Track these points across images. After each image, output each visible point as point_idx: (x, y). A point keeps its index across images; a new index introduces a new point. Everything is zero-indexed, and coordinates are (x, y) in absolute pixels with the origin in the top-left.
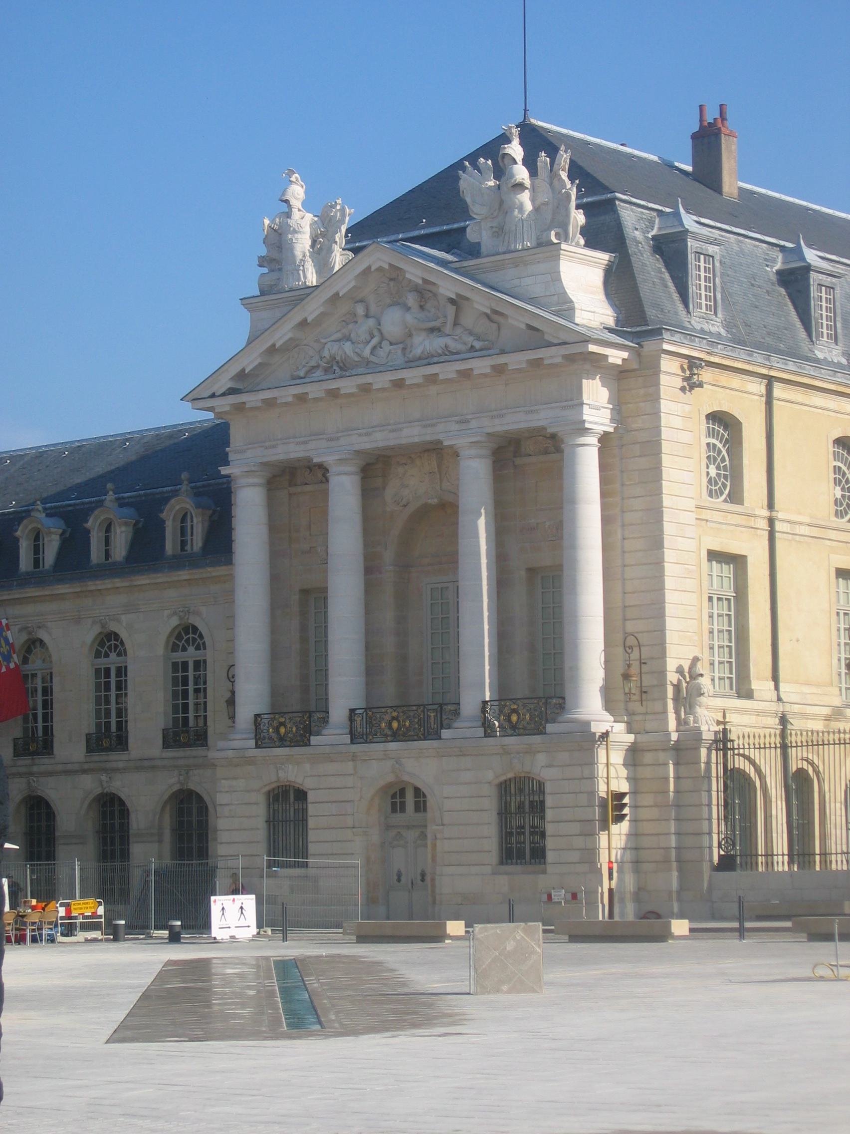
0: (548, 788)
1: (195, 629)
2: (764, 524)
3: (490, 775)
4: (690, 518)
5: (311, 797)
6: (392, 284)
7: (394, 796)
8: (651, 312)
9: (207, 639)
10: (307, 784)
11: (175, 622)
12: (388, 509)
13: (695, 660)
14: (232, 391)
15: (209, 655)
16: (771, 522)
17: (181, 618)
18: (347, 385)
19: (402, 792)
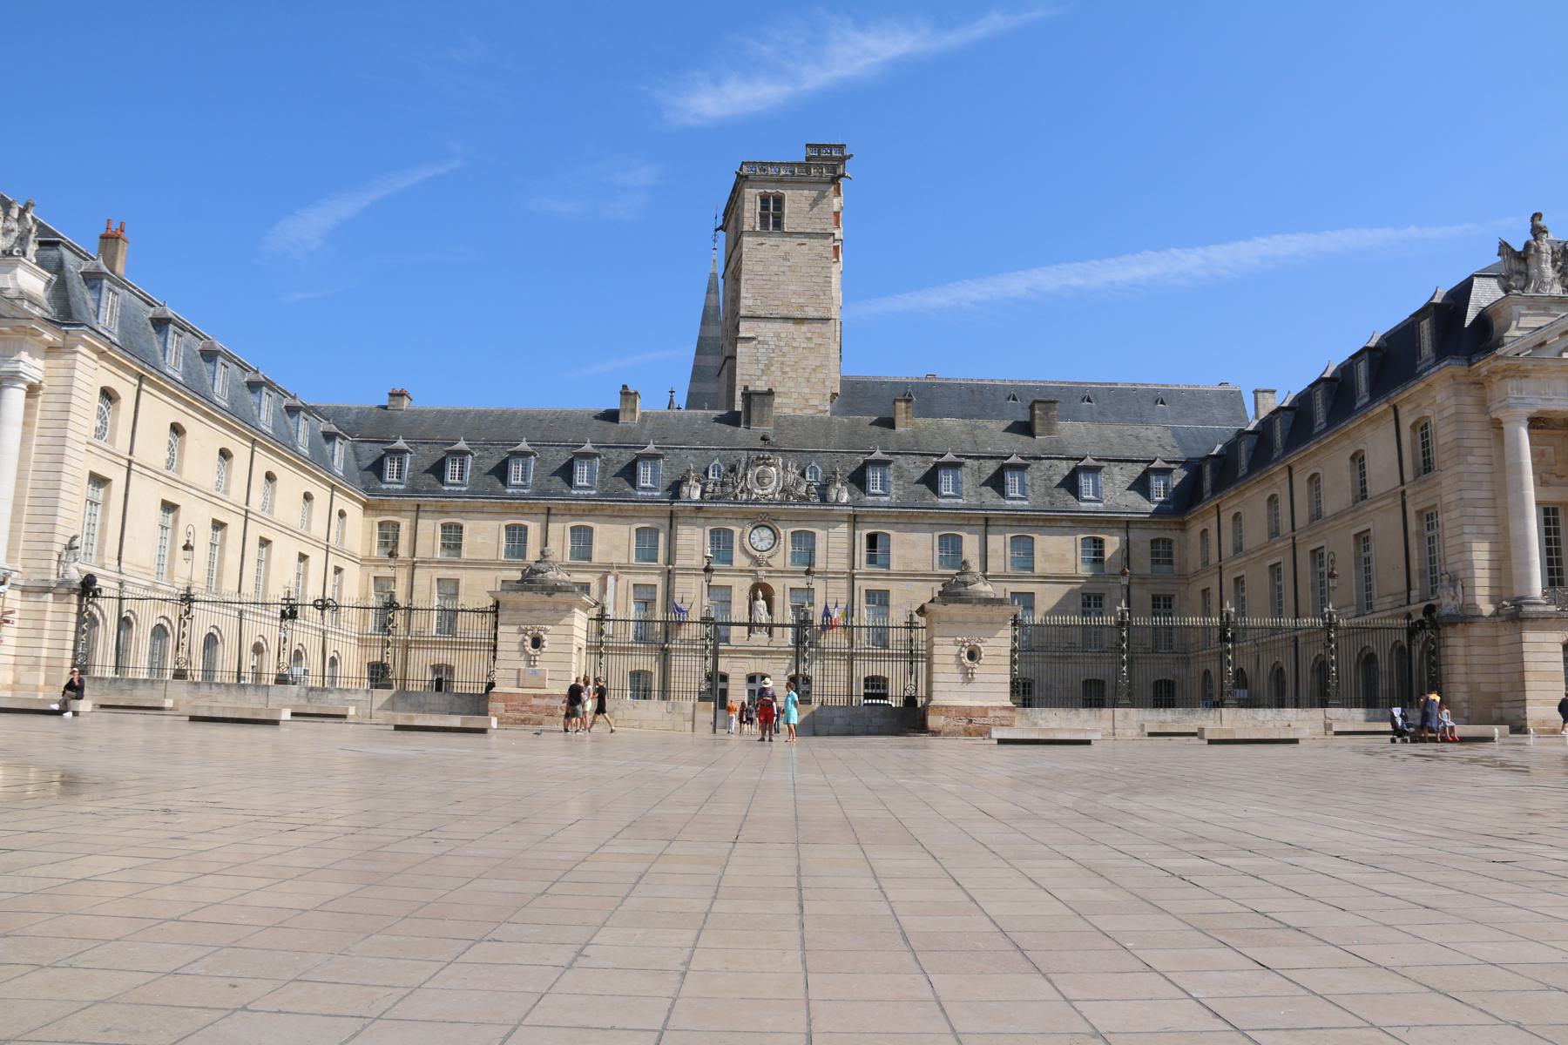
2: (125, 463)
4: (83, 448)
8: (75, 315)
13: (74, 538)
16: (130, 462)
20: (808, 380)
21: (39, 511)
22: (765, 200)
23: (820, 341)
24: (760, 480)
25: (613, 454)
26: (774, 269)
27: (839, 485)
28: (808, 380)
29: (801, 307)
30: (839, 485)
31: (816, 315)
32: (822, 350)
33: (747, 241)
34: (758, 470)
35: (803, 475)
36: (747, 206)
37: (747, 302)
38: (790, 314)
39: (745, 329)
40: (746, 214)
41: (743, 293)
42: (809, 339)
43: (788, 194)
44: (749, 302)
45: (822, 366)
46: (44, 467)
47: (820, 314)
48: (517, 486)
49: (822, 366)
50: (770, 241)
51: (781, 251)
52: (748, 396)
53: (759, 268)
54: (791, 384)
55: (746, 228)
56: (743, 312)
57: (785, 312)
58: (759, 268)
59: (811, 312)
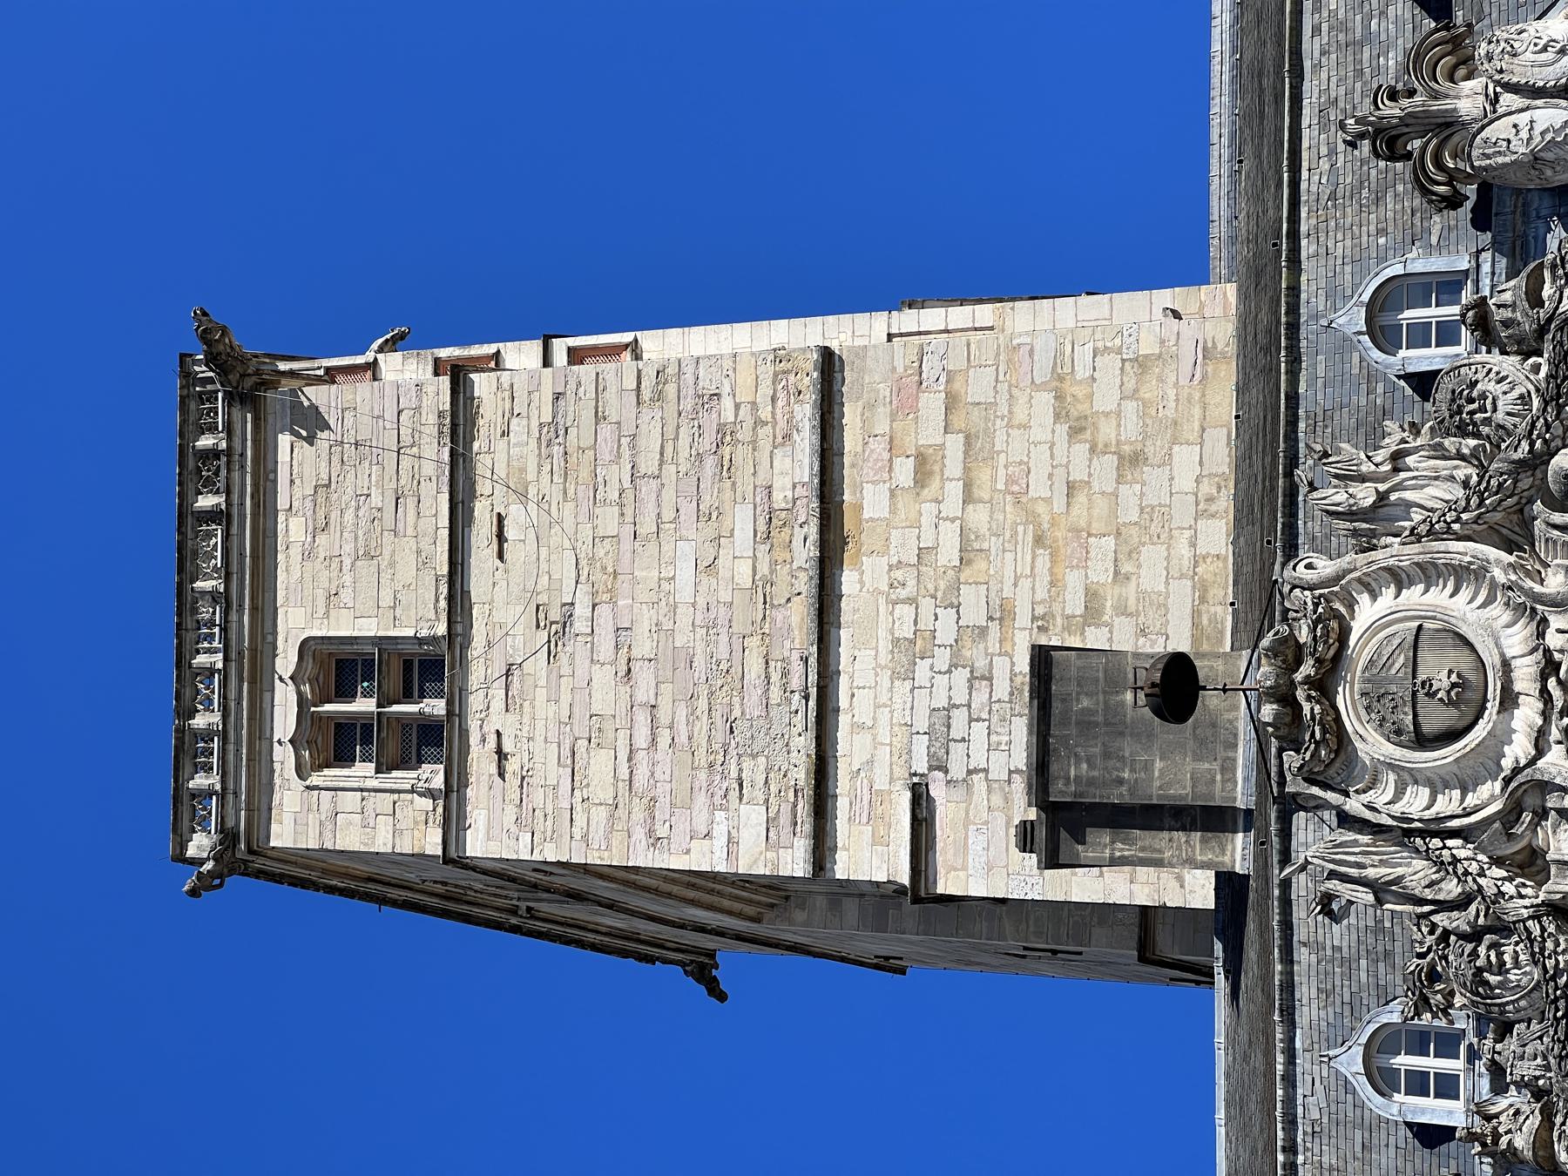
20: (1131, 461)
22: (334, 744)
23: (932, 404)
24: (1444, 713)
26: (605, 694)
27: (1467, 99)
28: (1131, 461)
29: (771, 525)
30: (1467, 99)
31: (806, 440)
32: (978, 387)
33: (490, 837)
34: (1372, 745)
35: (1423, 383)
37: (749, 839)
38: (805, 584)
39: (871, 854)
40: (382, 843)
41: (707, 858)
42: (924, 468)
43: (296, 623)
44: (753, 817)
45: (1058, 383)
47: (806, 412)
49: (1058, 383)
50: (486, 714)
51: (523, 640)
52: (1059, 827)
53: (600, 767)
54: (1150, 571)
55: (432, 843)
56: (794, 862)
57: (798, 616)
59: (795, 468)
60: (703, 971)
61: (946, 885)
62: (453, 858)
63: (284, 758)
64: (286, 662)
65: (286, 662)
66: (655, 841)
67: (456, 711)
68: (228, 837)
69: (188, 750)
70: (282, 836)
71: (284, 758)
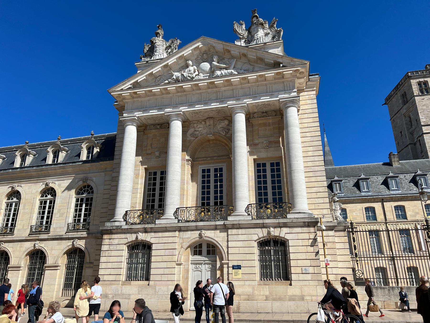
0: (291, 243)
1: (89, 186)
3: (256, 237)
5: (154, 247)
6: (205, 55)
7: (196, 247)
9: (95, 190)
10: (152, 241)
11: (81, 183)
12: (188, 139)
14: (130, 88)
15: (94, 196)
17: (84, 182)
18: (187, 86)
19: (200, 246)
21: (313, 179)
22: (419, 84)
25: (401, 176)
36: (413, 87)
37: (423, 120)
40: (414, 90)
44: (425, 120)
46: (310, 154)
48: (366, 192)
53: (425, 107)
55: (415, 94)
56: (422, 124)
58: (425, 107)
60: (385, 104)
61: (424, 135)
62: (414, 96)
63: (418, 80)
64: (426, 79)
65: (426, 79)
66: (421, 112)
67: (426, 95)
68: (411, 77)
69: (417, 72)
70: (412, 81)
71: (418, 80)
